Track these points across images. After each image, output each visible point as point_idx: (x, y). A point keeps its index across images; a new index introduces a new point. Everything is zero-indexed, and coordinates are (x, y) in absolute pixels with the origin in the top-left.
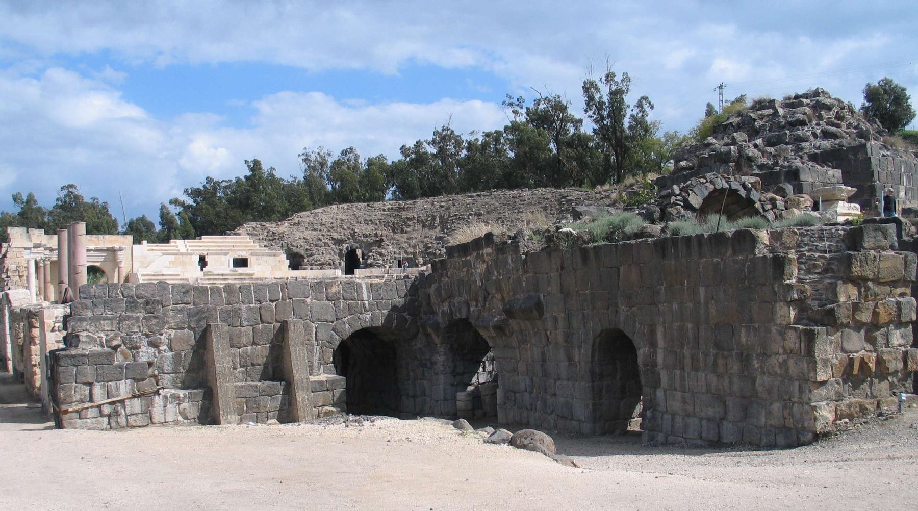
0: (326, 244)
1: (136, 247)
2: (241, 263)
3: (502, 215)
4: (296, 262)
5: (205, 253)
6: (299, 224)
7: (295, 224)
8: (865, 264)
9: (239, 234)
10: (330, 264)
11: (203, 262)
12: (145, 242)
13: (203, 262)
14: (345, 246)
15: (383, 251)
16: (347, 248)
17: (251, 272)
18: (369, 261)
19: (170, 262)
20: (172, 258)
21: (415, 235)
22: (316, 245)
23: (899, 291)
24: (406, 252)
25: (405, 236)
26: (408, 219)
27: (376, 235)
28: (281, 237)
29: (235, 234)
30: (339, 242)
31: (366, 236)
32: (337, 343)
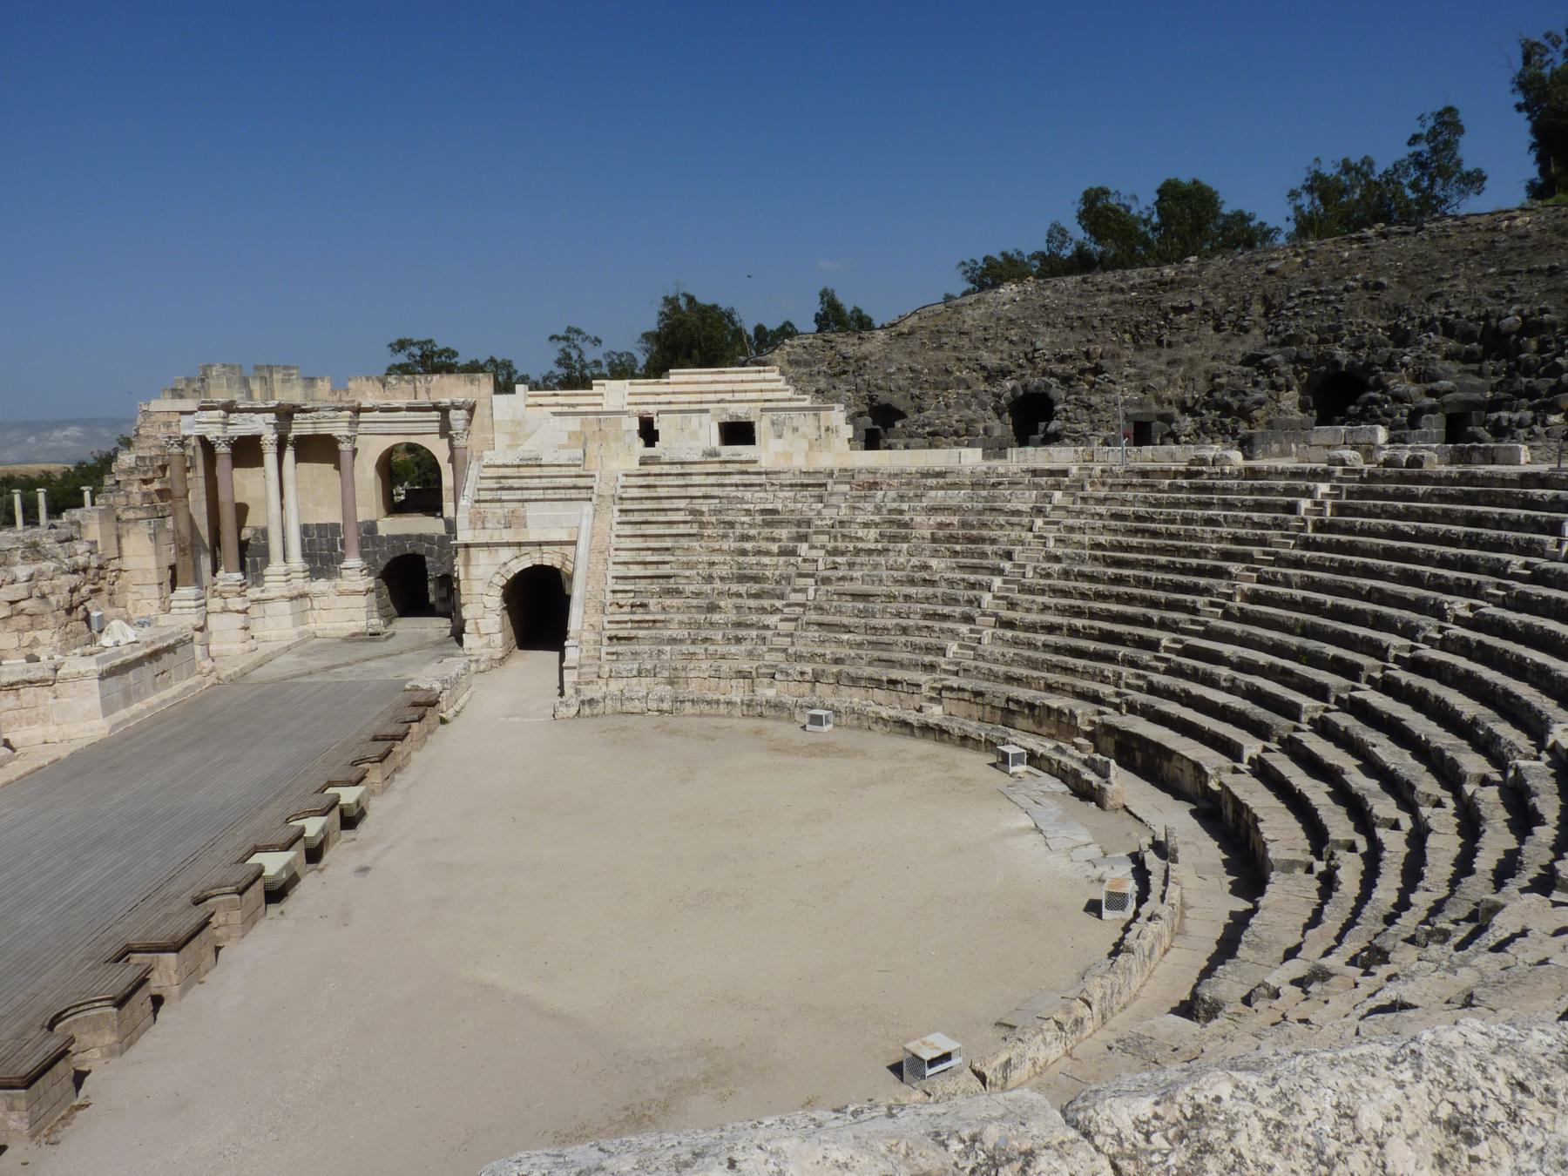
0: (961, 382)
1: (501, 400)
2: (738, 432)
3: (1445, 287)
4: (879, 425)
5: (652, 409)
6: (910, 333)
7: (901, 334)
9: (765, 364)
10: (956, 433)
11: (649, 433)
13: (649, 433)
14: (1009, 384)
15: (1095, 399)
16: (1014, 389)
17: (753, 457)
18: (1054, 425)
19: (571, 435)
20: (574, 424)
21: (1187, 351)
22: (936, 385)
24: (1159, 401)
25: (1166, 353)
26: (1178, 311)
27: (1087, 354)
28: (861, 362)
30: (993, 376)
31: (1062, 359)
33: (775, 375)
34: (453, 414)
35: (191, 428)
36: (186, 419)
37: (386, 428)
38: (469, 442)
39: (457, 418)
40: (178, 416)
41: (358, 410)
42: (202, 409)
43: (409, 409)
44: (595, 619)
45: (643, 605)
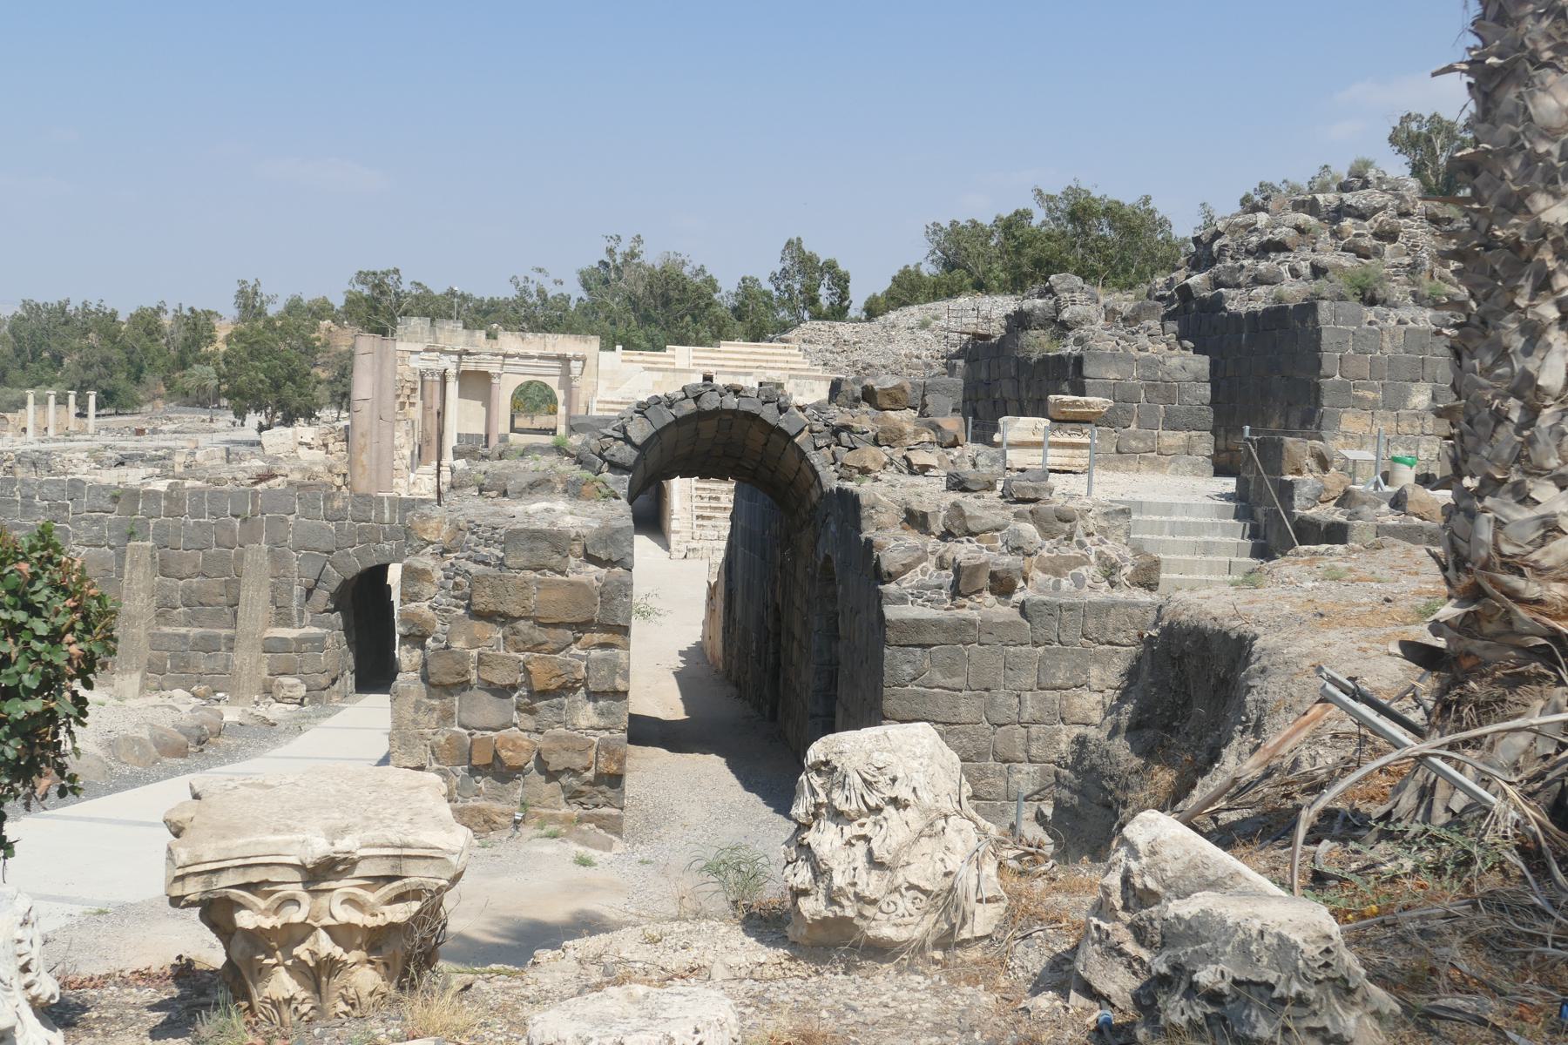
1: (606, 356)
5: (713, 370)
8: (501, 591)
9: (787, 341)
12: (619, 348)
23: (586, 637)
29: (782, 341)
32: (336, 584)
33: (796, 352)
34: (573, 363)
35: (416, 363)
36: (414, 357)
37: (523, 370)
38: (582, 385)
39: (575, 366)
40: (407, 355)
41: (505, 356)
42: (426, 350)
43: (541, 357)
44: (687, 505)
45: (717, 499)
